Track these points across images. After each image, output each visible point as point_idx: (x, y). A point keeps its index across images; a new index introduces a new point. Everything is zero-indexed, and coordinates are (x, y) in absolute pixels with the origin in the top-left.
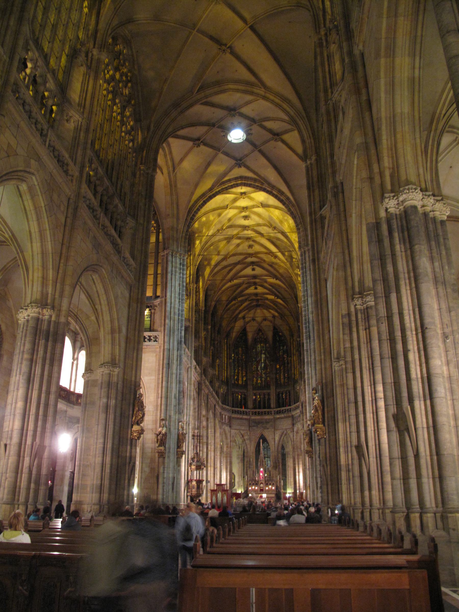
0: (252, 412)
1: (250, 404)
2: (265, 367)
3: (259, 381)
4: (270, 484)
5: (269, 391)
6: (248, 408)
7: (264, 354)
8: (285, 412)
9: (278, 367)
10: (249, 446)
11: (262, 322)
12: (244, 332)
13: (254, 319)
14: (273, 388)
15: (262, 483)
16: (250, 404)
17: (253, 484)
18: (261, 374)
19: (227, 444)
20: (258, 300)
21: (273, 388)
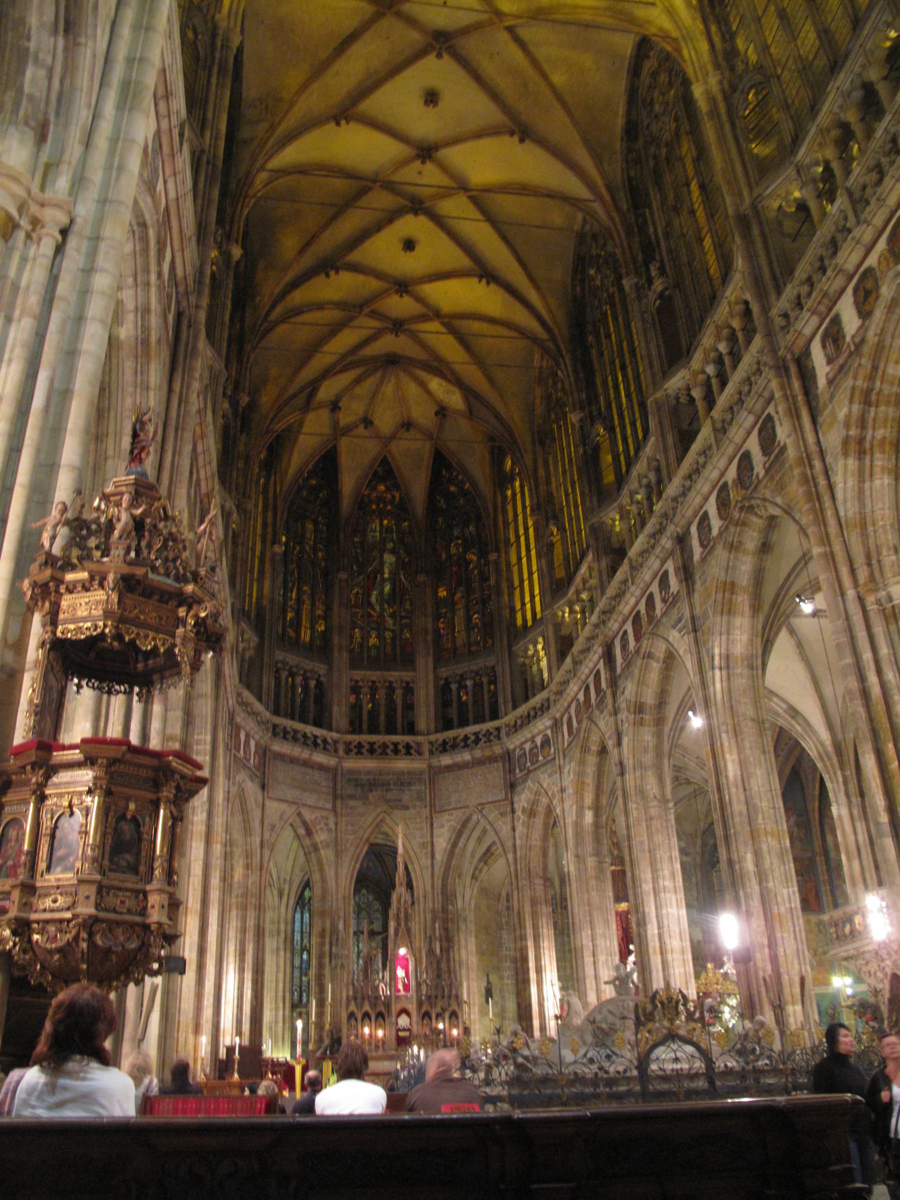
0: (348, 744)
1: (339, 713)
2: (395, 597)
3: (373, 641)
4: (439, 1016)
5: (407, 675)
6: (330, 729)
7: (393, 552)
8: (477, 741)
9: (443, 593)
10: (330, 873)
11: (393, 437)
12: (327, 464)
13: (367, 422)
14: (424, 663)
15: (405, 1011)
16: (339, 713)
17: (366, 1015)
18: (381, 615)
19: (248, 855)
20: (398, 326)
21: (424, 663)
